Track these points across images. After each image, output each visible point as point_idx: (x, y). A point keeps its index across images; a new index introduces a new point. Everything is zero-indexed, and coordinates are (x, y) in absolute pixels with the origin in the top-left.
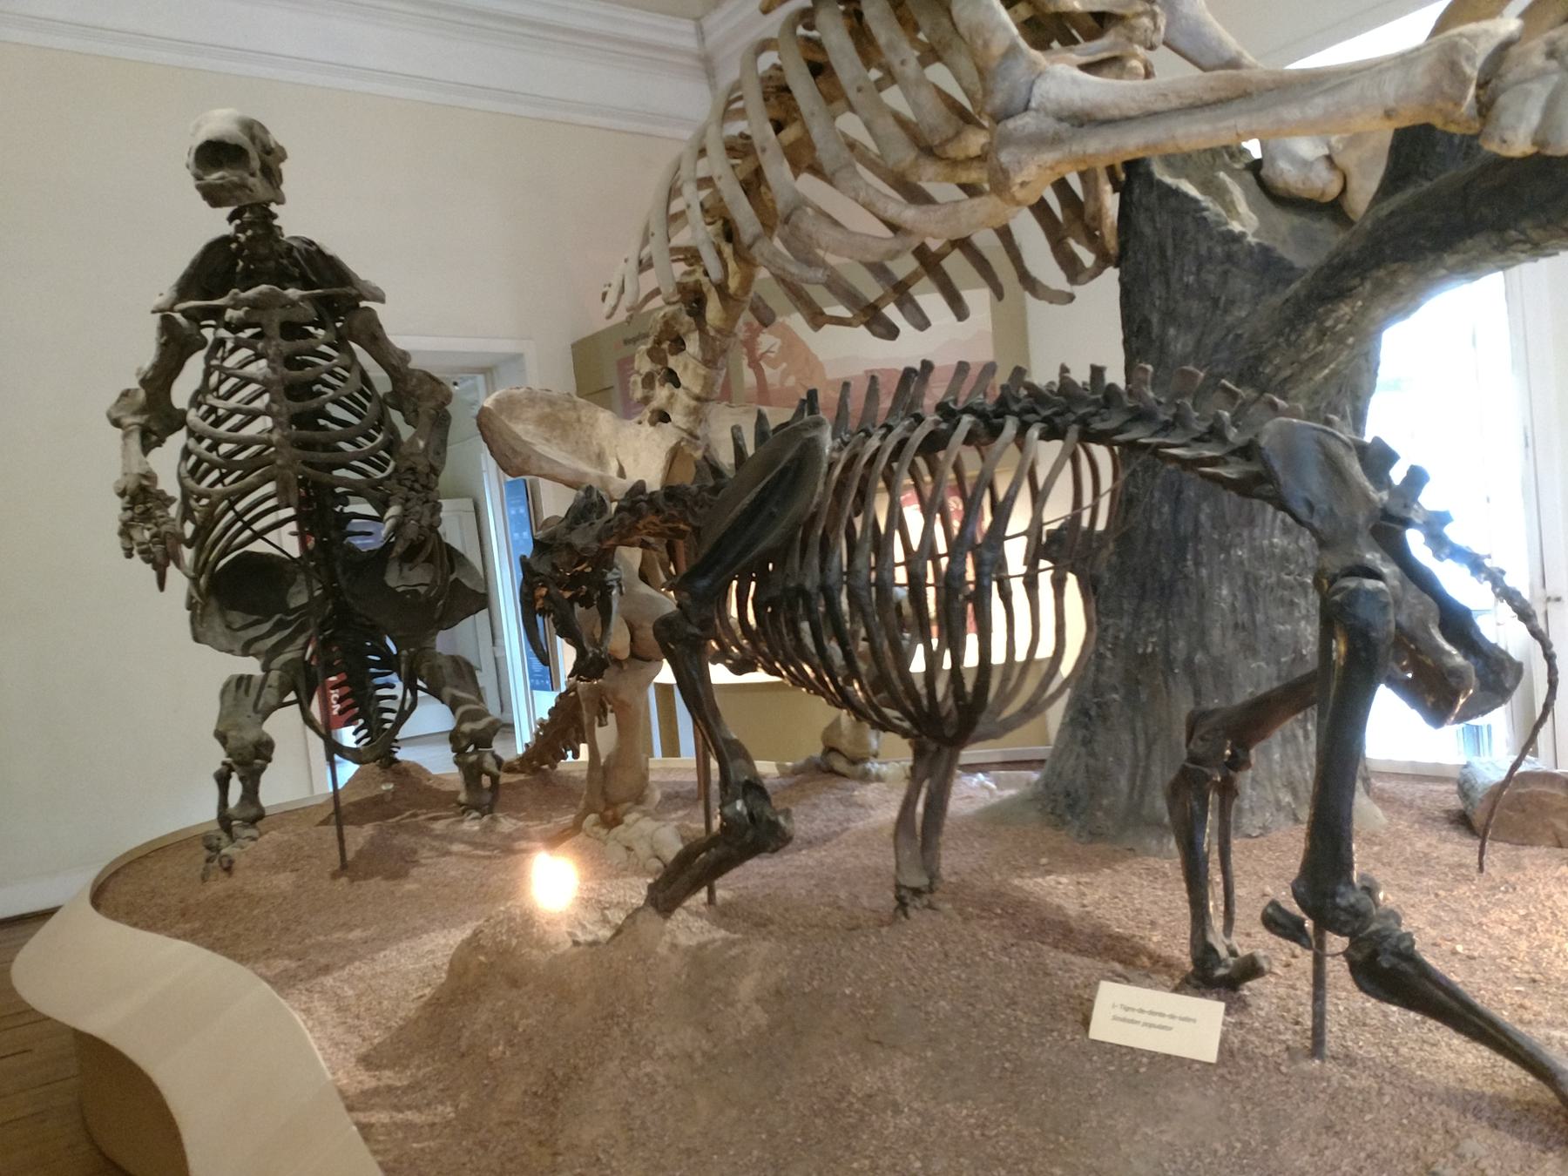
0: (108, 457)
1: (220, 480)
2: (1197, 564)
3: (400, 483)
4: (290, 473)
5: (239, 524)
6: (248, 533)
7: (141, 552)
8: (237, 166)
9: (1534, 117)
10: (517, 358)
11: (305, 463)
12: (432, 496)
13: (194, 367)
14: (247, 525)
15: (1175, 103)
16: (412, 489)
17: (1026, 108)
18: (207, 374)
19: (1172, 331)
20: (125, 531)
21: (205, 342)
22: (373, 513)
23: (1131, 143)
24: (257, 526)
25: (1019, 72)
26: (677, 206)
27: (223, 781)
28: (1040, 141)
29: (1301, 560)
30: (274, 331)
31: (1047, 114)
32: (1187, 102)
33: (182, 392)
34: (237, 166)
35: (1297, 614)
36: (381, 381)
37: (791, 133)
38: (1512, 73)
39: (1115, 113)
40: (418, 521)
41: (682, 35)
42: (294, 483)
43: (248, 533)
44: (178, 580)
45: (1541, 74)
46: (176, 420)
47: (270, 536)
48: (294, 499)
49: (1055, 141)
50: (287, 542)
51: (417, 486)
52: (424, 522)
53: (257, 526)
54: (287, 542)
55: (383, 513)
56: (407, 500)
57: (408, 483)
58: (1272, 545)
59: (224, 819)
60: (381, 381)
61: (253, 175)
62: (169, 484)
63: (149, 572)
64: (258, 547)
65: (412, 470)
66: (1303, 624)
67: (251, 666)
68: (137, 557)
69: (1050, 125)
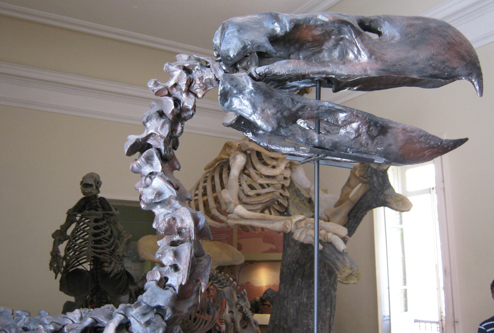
1: (74, 254)
2: (287, 304)
3: (115, 259)
4: (90, 254)
5: (76, 261)
6: (78, 263)
7: (53, 270)
8: (91, 184)
9: (298, 235)
11: (94, 252)
12: (122, 262)
13: (73, 226)
14: (78, 262)
15: (255, 218)
16: (118, 260)
17: (233, 213)
18: (76, 227)
19: (288, 249)
20: (51, 265)
21: (76, 221)
22: (108, 266)
24: (81, 262)
25: (232, 206)
26: (197, 192)
28: (234, 219)
29: (310, 305)
30: (92, 221)
31: (236, 215)
32: (257, 218)
33: (69, 232)
34: (91, 184)
35: (309, 318)
37: (205, 198)
38: (299, 226)
39: (246, 217)
40: (118, 269)
42: (90, 256)
43: (78, 263)
44: (60, 276)
45: (302, 227)
46: (66, 238)
47: (84, 265)
48: (90, 260)
49: (237, 220)
50: (87, 267)
51: (119, 260)
52: (119, 269)
53: (81, 262)
54: (87, 267)
55: (110, 265)
56: (116, 263)
57: (117, 259)
58: (303, 301)
61: (93, 190)
62: (62, 254)
63: (54, 274)
65: (118, 256)
66: (310, 321)
67: (72, 299)
68: (52, 271)
69: (236, 217)
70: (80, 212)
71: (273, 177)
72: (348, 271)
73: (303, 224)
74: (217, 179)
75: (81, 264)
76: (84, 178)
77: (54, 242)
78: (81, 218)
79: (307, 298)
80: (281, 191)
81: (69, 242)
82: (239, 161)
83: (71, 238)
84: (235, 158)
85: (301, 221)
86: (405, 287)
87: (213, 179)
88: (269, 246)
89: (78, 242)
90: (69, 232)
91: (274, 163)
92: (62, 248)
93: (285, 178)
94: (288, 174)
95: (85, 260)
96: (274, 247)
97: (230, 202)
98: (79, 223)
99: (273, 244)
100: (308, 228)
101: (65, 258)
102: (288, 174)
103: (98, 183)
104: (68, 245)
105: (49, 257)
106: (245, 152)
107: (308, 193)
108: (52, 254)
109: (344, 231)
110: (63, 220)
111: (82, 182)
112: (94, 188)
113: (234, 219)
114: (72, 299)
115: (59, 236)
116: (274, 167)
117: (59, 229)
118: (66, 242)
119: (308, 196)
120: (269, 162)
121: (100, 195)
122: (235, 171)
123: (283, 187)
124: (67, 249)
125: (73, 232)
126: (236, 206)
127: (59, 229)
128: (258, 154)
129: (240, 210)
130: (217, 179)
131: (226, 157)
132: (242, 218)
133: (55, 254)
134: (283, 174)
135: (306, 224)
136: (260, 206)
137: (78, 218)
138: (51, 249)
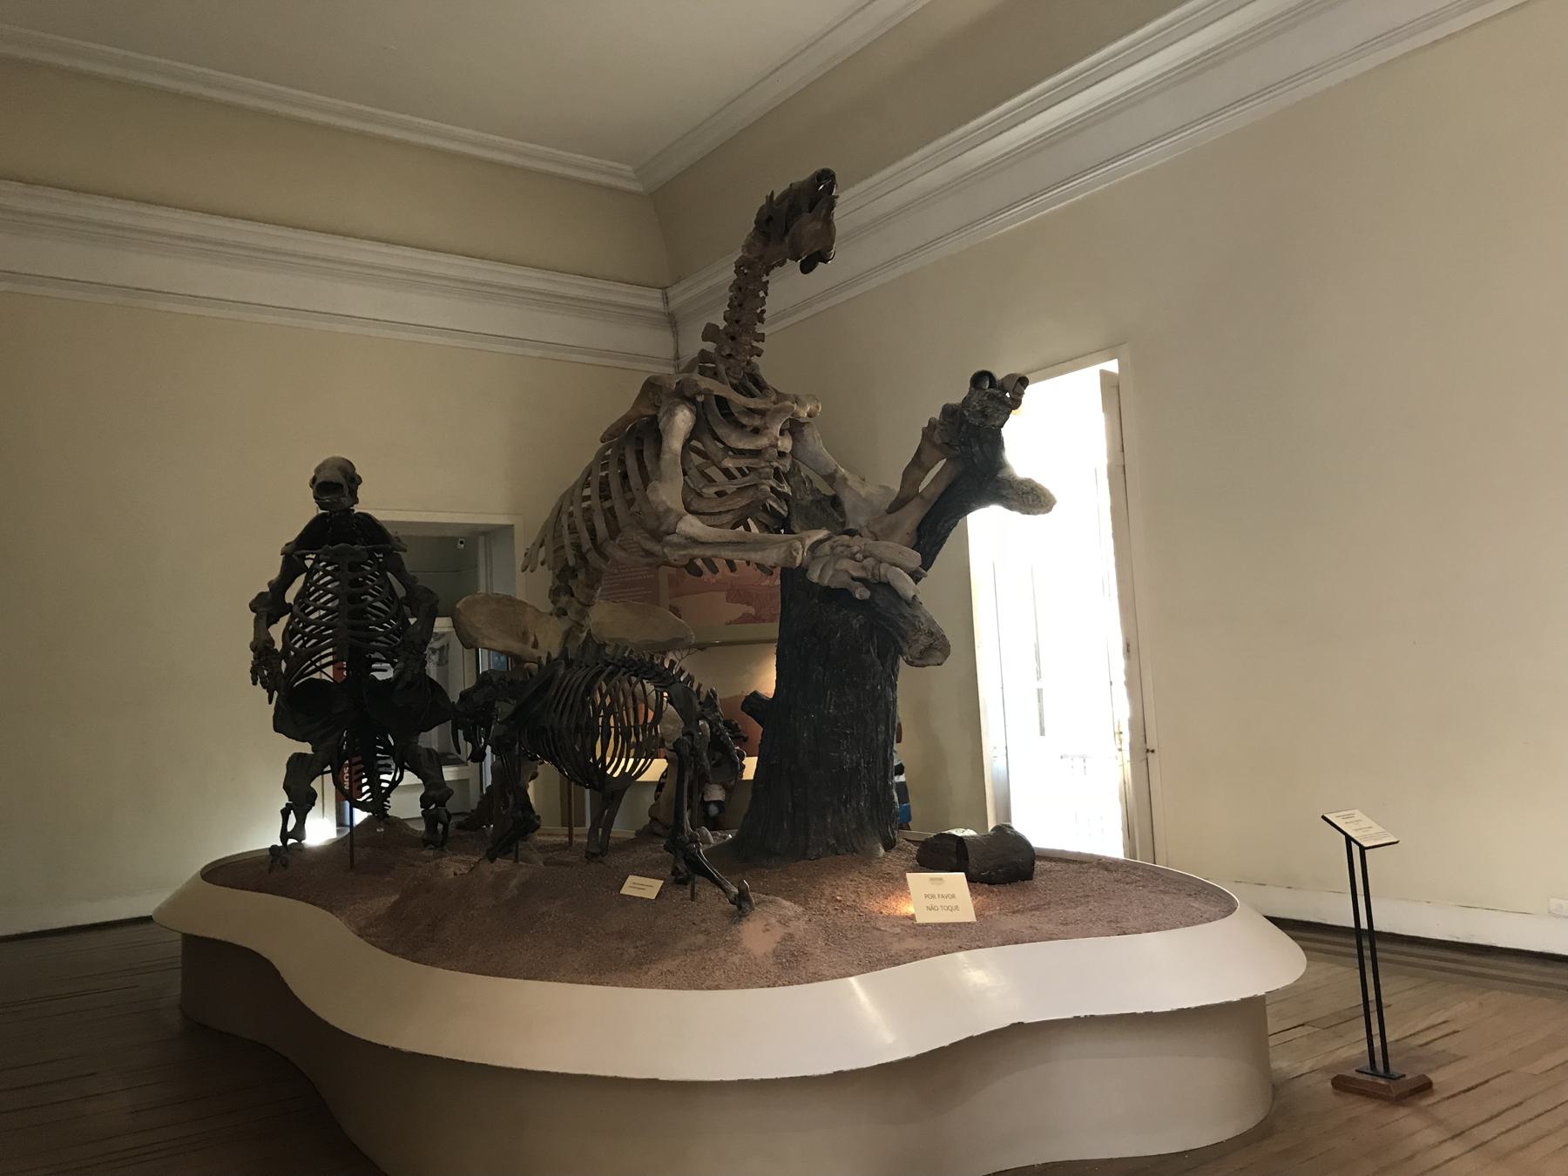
0: (245, 626)
8: (336, 485)
10: (508, 529)
13: (300, 581)
14: (313, 663)
20: (255, 672)
21: (303, 569)
23: (709, 553)
25: (672, 518)
27: (285, 814)
28: (679, 546)
33: (290, 597)
34: (336, 485)
36: (401, 592)
38: (818, 553)
41: (651, 300)
49: (685, 547)
59: (285, 835)
60: (401, 592)
63: (265, 694)
64: (316, 676)
67: (306, 748)
69: (683, 541)
70: (312, 549)
71: (756, 453)
72: (924, 640)
73: (827, 547)
74: (631, 463)
75: (319, 669)
76: (318, 470)
77: (256, 620)
78: (317, 561)
79: (836, 707)
80: (773, 483)
81: (293, 618)
82: (683, 419)
83: (296, 609)
84: (671, 414)
85: (821, 542)
86: (1040, 685)
87: (622, 462)
88: (739, 610)
89: (313, 617)
90: (290, 597)
91: (757, 422)
92: (277, 631)
93: (782, 454)
94: (786, 444)
95: (330, 658)
96: (752, 610)
97: (669, 510)
98: (311, 572)
99: (748, 604)
100: (840, 557)
101: (284, 654)
102: (786, 444)
103: (354, 481)
104: (289, 624)
105: (250, 656)
106: (690, 400)
107: (831, 486)
108: (254, 648)
109: (914, 559)
110: (274, 571)
111: (314, 480)
112: (346, 492)
113: (679, 546)
114: (306, 748)
115: (268, 606)
116: (756, 431)
117: (267, 589)
118: (284, 620)
119: (829, 492)
120: (744, 420)
121: (357, 509)
122: (675, 443)
123: (777, 474)
124: (289, 634)
125: (301, 596)
126: (680, 517)
127: (267, 589)
128: (722, 402)
129: (691, 525)
130: (631, 463)
131: (651, 412)
132: (695, 541)
133: (262, 651)
134: (776, 446)
135: (832, 548)
136: (728, 518)
137: (309, 563)
138: (250, 636)
